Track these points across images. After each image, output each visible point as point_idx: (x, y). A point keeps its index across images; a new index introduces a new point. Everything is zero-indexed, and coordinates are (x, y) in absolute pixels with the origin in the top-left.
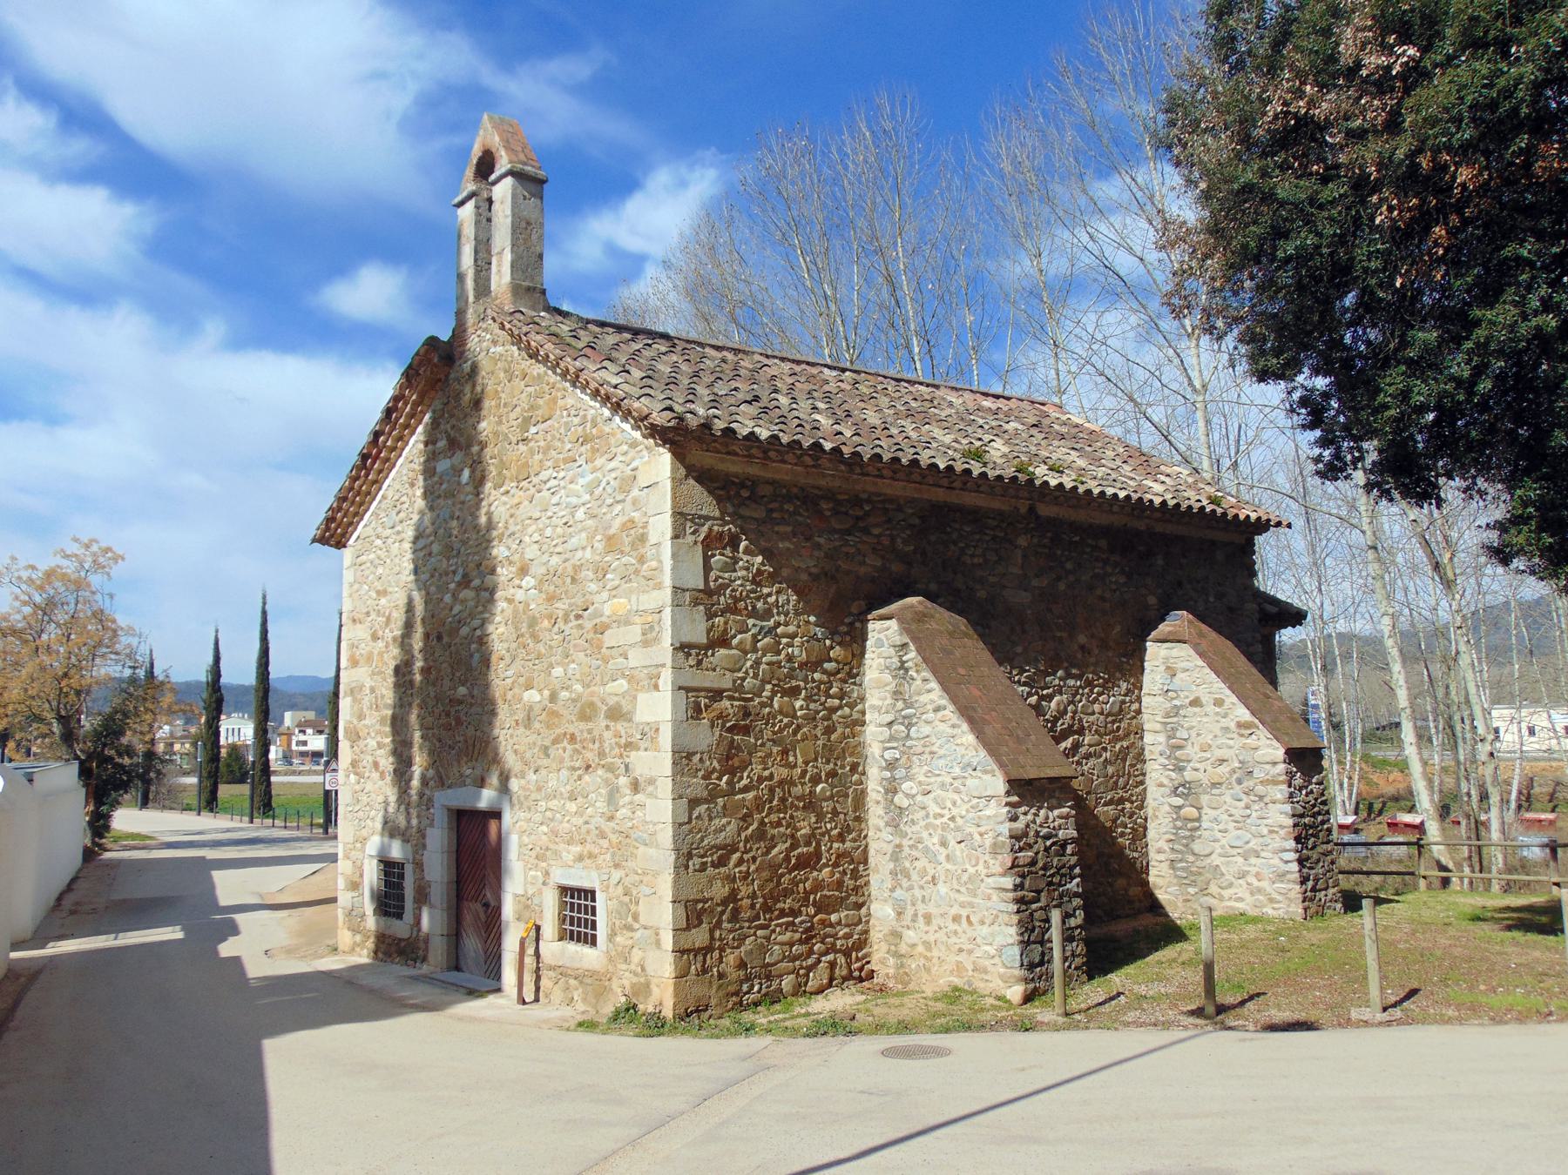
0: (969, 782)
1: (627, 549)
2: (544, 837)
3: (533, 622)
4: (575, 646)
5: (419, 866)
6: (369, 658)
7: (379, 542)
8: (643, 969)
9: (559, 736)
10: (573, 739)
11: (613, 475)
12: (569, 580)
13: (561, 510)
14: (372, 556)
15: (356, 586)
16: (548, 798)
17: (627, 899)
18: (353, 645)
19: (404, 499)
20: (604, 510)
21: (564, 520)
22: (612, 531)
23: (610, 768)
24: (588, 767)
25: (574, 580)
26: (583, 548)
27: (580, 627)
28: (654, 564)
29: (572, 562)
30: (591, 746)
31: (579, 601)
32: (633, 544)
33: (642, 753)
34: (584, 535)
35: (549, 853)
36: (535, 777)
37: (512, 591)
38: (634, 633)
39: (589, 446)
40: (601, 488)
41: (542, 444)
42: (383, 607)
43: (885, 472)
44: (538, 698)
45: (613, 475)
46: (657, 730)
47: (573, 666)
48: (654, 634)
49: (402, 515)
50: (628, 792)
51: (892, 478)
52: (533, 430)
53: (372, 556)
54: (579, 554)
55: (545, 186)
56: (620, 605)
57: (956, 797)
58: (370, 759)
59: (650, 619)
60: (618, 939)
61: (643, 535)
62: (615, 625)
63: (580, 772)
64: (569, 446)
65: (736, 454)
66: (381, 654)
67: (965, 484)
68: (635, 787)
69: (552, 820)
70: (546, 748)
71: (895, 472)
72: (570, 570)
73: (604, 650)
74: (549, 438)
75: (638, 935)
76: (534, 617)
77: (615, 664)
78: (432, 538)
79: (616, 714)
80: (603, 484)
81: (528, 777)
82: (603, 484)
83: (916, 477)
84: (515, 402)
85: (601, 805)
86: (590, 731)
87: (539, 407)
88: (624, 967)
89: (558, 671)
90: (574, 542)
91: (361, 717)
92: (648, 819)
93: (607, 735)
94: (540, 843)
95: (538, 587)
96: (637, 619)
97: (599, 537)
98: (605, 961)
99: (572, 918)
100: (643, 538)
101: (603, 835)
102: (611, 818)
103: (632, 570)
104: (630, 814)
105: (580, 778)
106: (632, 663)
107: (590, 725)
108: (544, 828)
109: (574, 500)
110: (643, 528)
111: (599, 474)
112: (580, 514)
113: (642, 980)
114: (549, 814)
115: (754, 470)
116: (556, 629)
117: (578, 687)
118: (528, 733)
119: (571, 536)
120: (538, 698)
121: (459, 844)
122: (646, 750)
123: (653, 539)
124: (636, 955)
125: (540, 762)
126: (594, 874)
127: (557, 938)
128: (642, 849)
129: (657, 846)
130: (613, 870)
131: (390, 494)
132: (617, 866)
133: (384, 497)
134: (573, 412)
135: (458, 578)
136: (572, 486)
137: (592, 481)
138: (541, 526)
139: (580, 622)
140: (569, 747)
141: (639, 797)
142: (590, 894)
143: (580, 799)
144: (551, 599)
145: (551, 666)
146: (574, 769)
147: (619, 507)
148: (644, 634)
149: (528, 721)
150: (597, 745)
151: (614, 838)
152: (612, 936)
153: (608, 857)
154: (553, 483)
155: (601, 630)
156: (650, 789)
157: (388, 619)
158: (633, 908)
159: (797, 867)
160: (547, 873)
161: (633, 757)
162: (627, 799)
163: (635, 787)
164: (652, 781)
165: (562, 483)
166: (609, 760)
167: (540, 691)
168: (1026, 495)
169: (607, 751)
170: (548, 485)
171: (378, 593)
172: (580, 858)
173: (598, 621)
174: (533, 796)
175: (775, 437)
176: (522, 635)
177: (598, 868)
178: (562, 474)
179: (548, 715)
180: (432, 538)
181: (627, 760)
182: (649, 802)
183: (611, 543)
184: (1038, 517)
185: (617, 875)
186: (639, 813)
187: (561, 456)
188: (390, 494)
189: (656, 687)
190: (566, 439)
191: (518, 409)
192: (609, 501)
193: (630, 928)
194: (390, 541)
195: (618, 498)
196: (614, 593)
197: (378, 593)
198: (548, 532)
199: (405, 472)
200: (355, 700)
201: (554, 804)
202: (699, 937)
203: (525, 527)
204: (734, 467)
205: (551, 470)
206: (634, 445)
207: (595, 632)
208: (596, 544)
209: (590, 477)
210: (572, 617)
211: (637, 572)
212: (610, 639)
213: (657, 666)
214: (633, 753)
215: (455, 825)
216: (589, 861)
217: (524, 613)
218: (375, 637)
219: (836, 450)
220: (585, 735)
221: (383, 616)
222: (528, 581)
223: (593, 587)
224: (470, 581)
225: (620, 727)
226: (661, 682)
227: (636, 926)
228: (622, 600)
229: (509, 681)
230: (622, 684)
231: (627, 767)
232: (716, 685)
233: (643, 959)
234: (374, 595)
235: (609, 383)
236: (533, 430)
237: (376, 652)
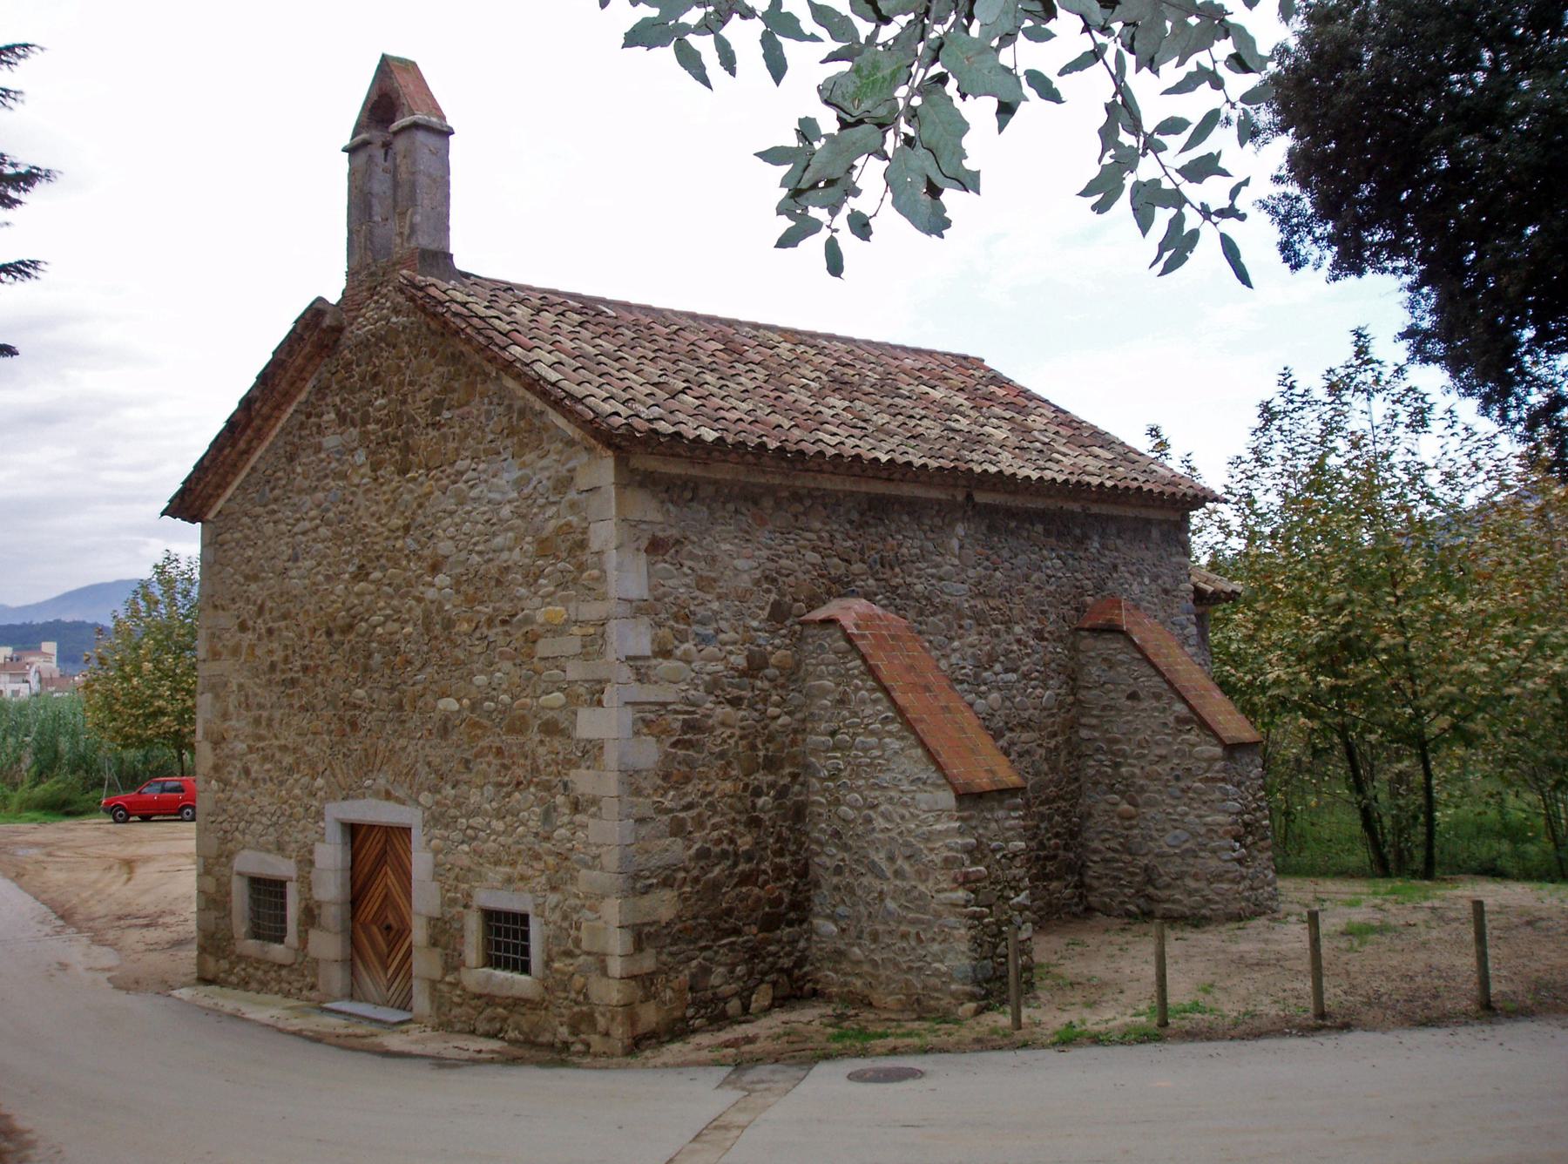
0: (919, 796)
1: (564, 555)
2: (464, 857)
3: (449, 624)
4: (501, 653)
5: (306, 882)
6: (235, 651)
7: (246, 520)
8: (586, 996)
9: (483, 748)
10: (500, 752)
11: (547, 474)
12: (493, 583)
13: (482, 505)
14: (238, 535)
15: (217, 568)
16: (469, 815)
17: (565, 924)
18: (213, 635)
19: (280, 474)
20: (535, 510)
21: (486, 517)
22: (545, 534)
23: (548, 787)
24: (519, 784)
25: (499, 582)
26: (511, 550)
27: (507, 633)
28: (596, 572)
29: (497, 562)
30: (522, 761)
31: (507, 607)
32: (570, 551)
33: (583, 771)
34: (510, 534)
35: (470, 875)
36: (453, 792)
37: (421, 588)
38: (571, 644)
39: (516, 439)
40: (531, 486)
41: (457, 430)
42: (254, 593)
43: (825, 467)
44: (456, 707)
45: (547, 474)
46: (601, 748)
47: (498, 674)
48: (597, 647)
49: (277, 492)
50: (567, 811)
51: (832, 473)
52: (447, 414)
53: (238, 535)
54: (505, 555)
55: (451, 137)
56: (557, 612)
57: (904, 812)
58: (239, 765)
59: (592, 631)
60: (557, 965)
61: (583, 540)
62: (549, 635)
63: (509, 789)
64: (491, 437)
65: (680, 456)
66: (252, 647)
67: (904, 475)
68: (576, 807)
69: (475, 838)
70: (467, 762)
71: (835, 467)
72: (494, 572)
73: (535, 660)
74: (466, 426)
75: (582, 959)
76: (449, 619)
77: (550, 675)
78: (318, 521)
79: (551, 728)
80: (534, 482)
81: (444, 793)
82: (534, 482)
83: (857, 470)
84: (422, 380)
85: (534, 824)
86: (522, 746)
87: (454, 390)
88: (563, 995)
89: (480, 679)
90: (499, 541)
91: (225, 716)
92: (591, 841)
93: (541, 750)
94: (459, 863)
95: (457, 584)
96: (575, 629)
97: (529, 539)
98: (541, 989)
99: (498, 943)
100: (582, 545)
101: (537, 857)
102: (547, 839)
103: (569, 577)
104: (568, 834)
105: (509, 795)
106: (572, 674)
107: (521, 739)
108: (465, 847)
109: (496, 496)
110: (582, 533)
111: (529, 471)
112: (506, 511)
113: (585, 1008)
114: (469, 832)
115: (696, 471)
116: (477, 634)
117: (505, 698)
118: (443, 744)
119: (495, 535)
120: (456, 707)
121: (353, 861)
122: (588, 768)
123: (595, 545)
124: (578, 981)
125: (460, 777)
126: (528, 896)
127: (481, 962)
128: (584, 872)
129: (602, 869)
130: (548, 894)
131: (262, 466)
132: (554, 889)
133: (254, 469)
134: (495, 400)
135: (352, 569)
136: (495, 480)
137: (521, 478)
138: (458, 520)
139: (507, 628)
140: (495, 761)
141: (579, 818)
142: (524, 918)
143: (509, 818)
144: (471, 601)
145: (472, 674)
146: (500, 785)
147: (554, 509)
148: (584, 646)
149: (445, 730)
150: (529, 762)
151: (551, 860)
152: (547, 964)
153: (543, 879)
154: (471, 474)
155: (532, 639)
156: (593, 809)
157: (261, 609)
158: (573, 932)
159: (740, 883)
160: (469, 895)
161: (573, 774)
162: (566, 819)
163: (576, 807)
164: (594, 801)
165: (484, 477)
166: (544, 777)
167: (459, 700)
168: (964, 483)
169: (542, 767)
170: (465, 477)
171: (247, 577)
172: (509, 880)
173: (528, 628)
174: (453, 812)
175: (721, 440)
176: (436, 638)
177: (532, 891)
178: (482, 466)
179: (468, 726)
180: (318, 521)
181: (566, 778)
182: (591, 822)
183: (545, 547)
184: (975, 505)
185: (553, 898)
186: (580, 834)
187: (482, 447)
188: (262, 466)
189: (600, 703)
190: (487, 430)
191: (428, 390)
192: (541, 501)
193: (568, 954)
194: (260, 520)
195: (552, 499)
196: (548, 600)
197: (247, 577)
198: (467, 527)
199: (281, 444)
200: (217, 696)
201: (478, 821)
202: (648, 962)
203: (438, 520)
204: (676, 469)
205: (469, 461)
206: (571, 443)
207: (526, 641)
208: (526, 547)
209: (517, 474)
210: (497, 622)
211: (575, 581)
212: (544, 648)
213: (599, 682)
214: (573, 773)
215: (348, 839)
216: (521, 884)
217: (438, 612)
218: (243, 627)
219: (781, 450)
220: (515, 749)
221: (255, 603)
222: (442, 579)
223: (523, 591)
224: (368, 574)
225: (557, 743)
226: (605, 698)
227: (577, 952)
228: (558, 608)
229: (419, 687)
230: (557, 698)
231: (565, 785)
232: (661, 699)
233: (585, 985)
234: (242, 580)
235: (545, 380)
236: (447, 414)
237: (245, 644)
